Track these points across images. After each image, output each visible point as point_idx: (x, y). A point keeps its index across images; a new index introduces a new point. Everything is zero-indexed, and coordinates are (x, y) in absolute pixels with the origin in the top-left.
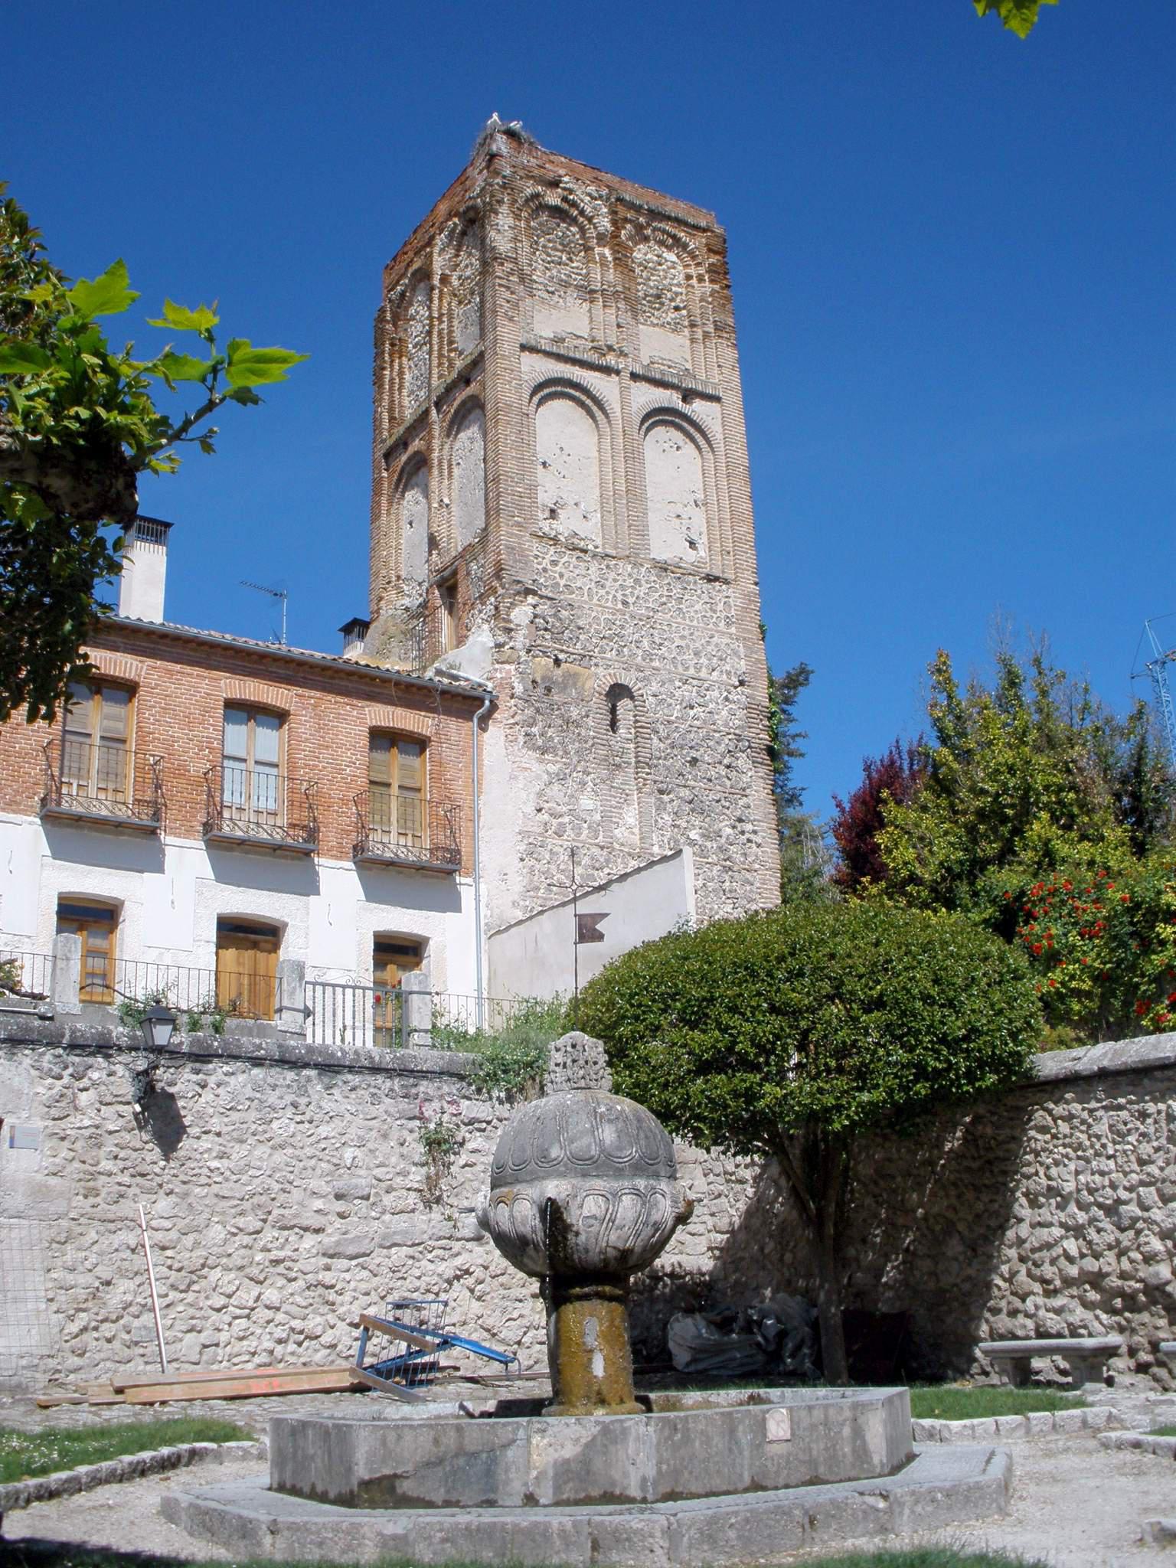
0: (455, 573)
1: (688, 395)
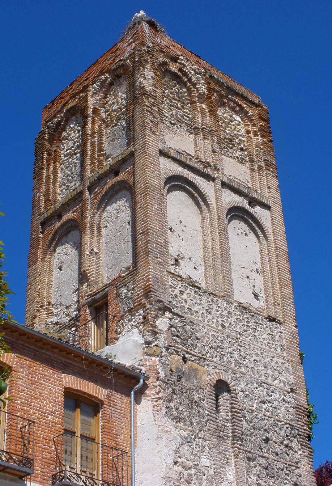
1: (253, 202)
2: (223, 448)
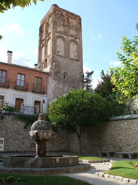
0: (47, 59)
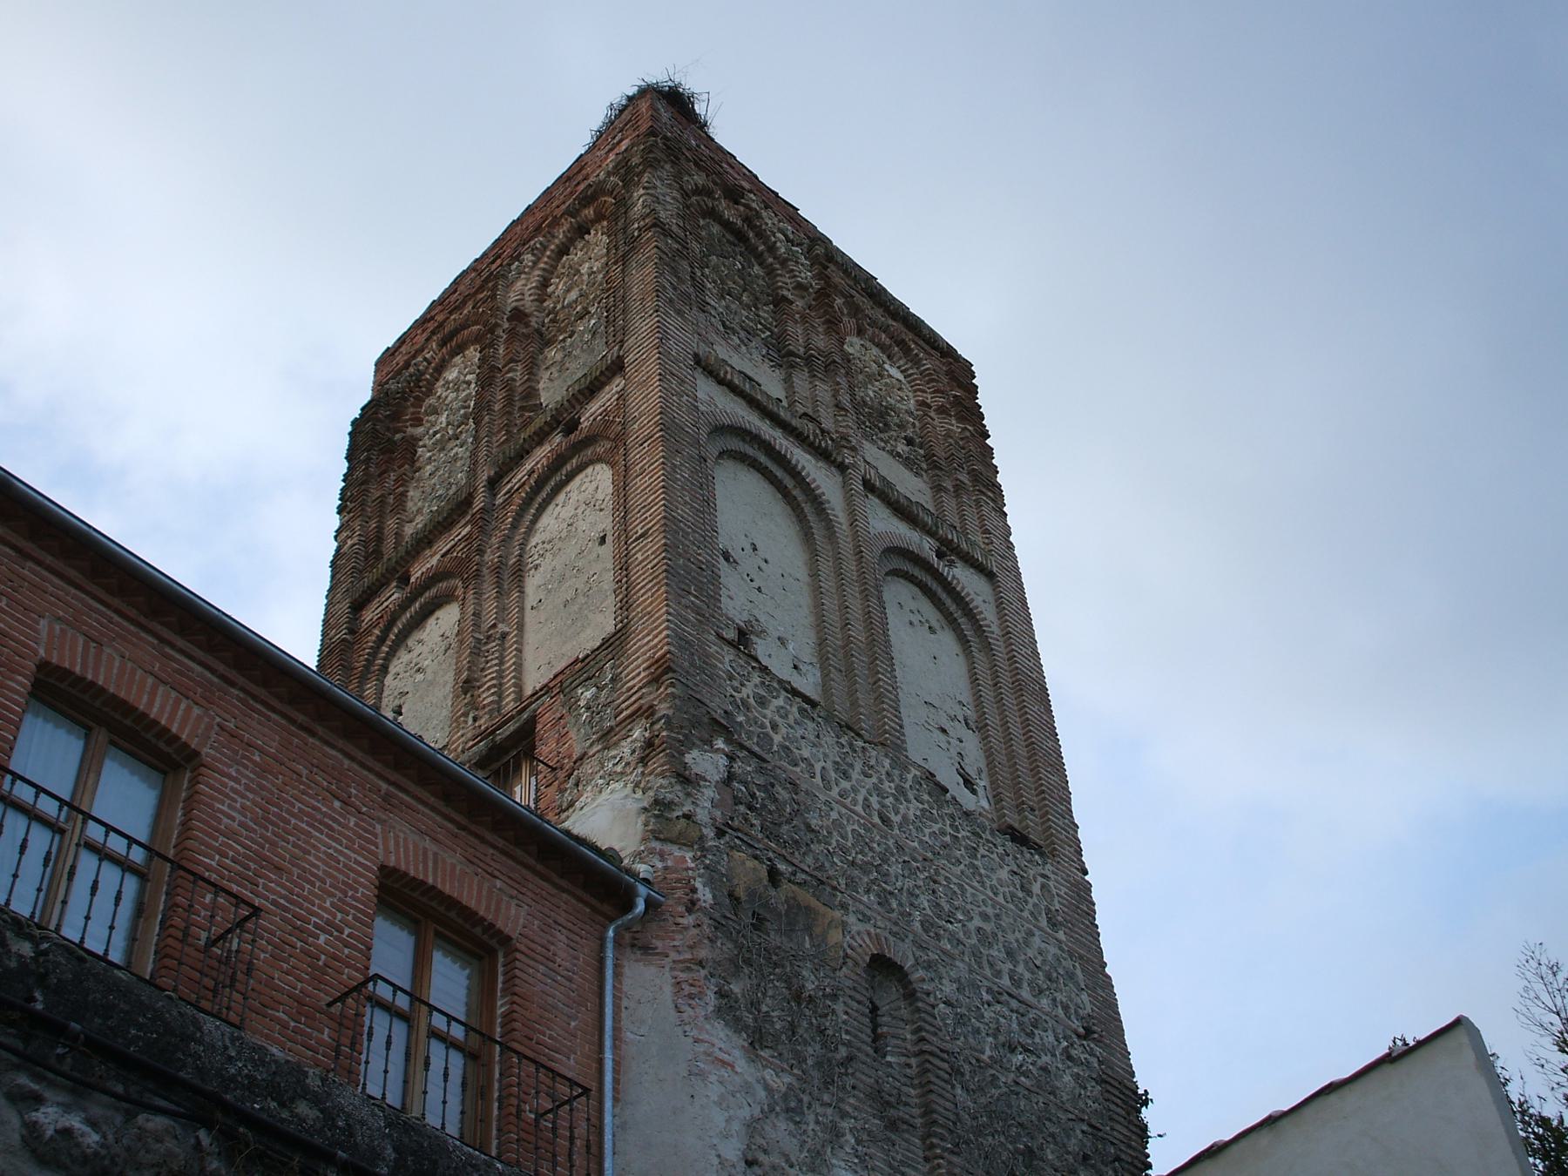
0: (533, 720)
1: (947, 549)
2: (899, 1157)
